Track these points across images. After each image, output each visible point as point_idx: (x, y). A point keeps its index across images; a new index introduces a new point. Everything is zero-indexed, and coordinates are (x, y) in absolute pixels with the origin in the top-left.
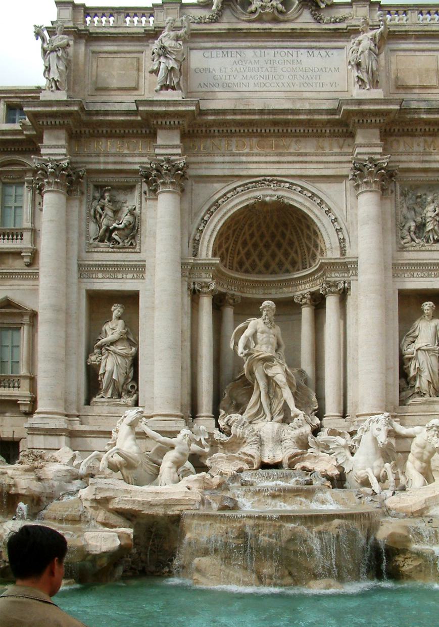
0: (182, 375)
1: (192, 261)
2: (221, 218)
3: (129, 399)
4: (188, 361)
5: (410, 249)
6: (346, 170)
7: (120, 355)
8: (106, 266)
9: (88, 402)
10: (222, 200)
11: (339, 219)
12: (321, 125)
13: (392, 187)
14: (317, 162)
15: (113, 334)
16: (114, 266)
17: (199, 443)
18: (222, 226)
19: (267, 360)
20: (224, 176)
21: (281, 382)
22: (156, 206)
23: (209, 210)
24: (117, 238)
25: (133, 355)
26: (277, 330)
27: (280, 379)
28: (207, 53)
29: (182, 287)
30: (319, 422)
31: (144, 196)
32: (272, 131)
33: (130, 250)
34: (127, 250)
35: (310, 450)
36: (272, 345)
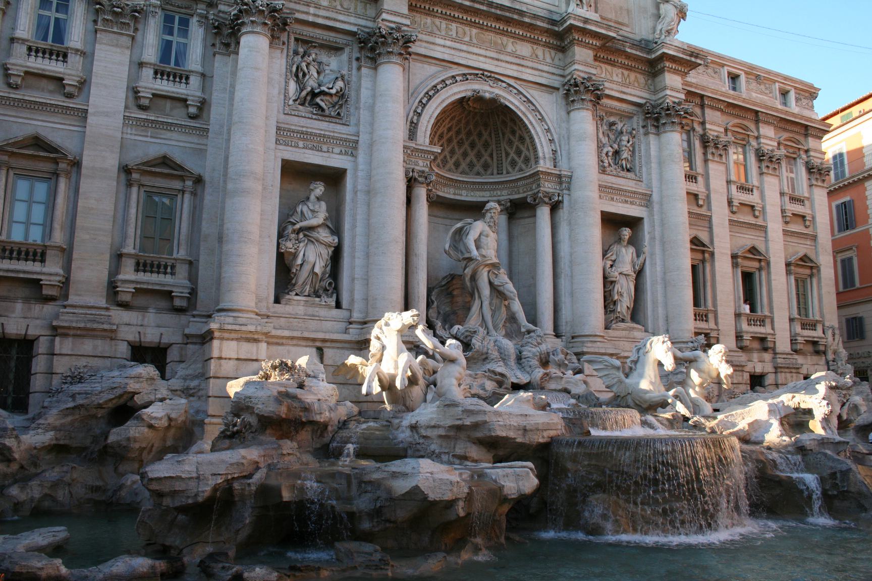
3: (330, 299)
6: (556, 82)
9: (277, 301)
10: (441, 86)
14: (533, 68)
16: (320, 135)
23: (427, 93)
24: (322, 104)
34: (334, 120)
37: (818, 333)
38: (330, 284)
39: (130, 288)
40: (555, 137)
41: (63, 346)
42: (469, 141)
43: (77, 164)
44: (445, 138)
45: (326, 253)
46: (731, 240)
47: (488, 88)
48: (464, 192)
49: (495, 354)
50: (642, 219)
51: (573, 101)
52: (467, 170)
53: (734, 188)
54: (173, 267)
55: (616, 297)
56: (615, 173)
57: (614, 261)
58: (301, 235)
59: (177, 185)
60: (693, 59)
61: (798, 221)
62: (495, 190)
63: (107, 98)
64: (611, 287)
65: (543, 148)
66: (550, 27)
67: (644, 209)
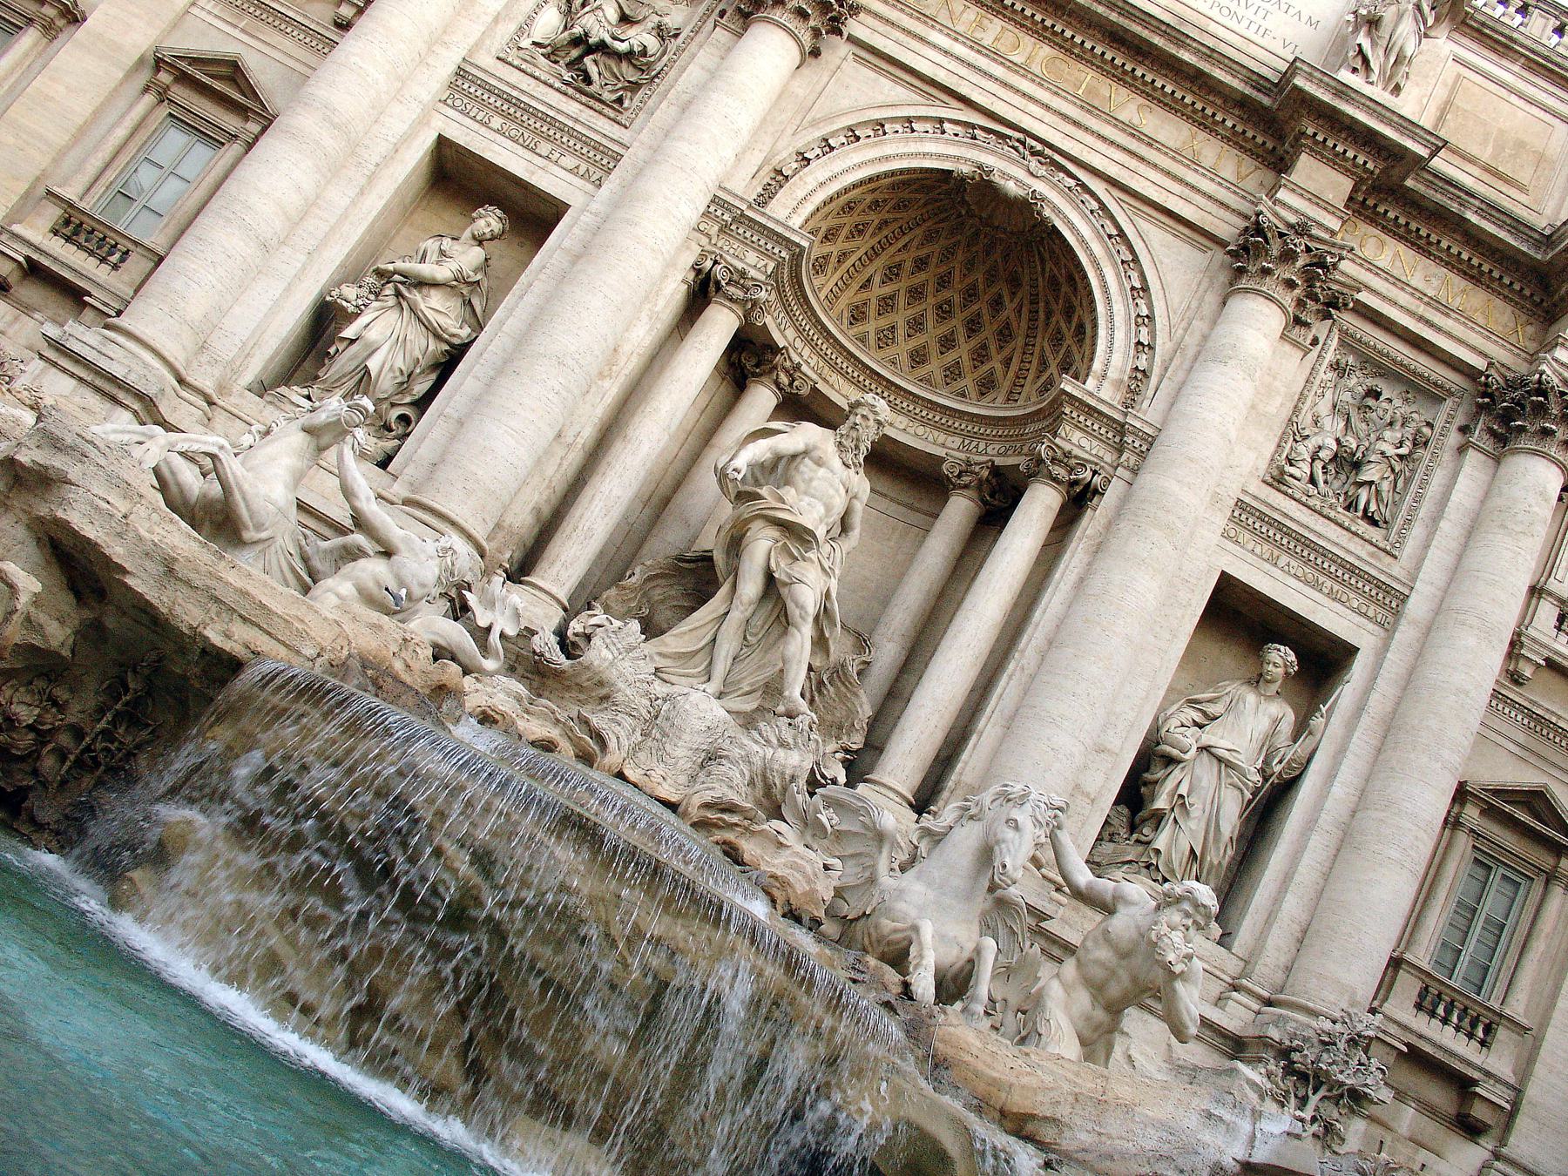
0: (548, 452)
1: (744, 207)
2: (872, 161)
4: (586, 432)
5: (1297, 496)
6: (1227, 227)
8: (527, 109)
9: (262, 389)
10: (898, 127)
11: (1158, 326)
12: (1219, 102)
13: (1320, 329)
14: (1168, 174)
15: (437, 263)
16: (544, 118)
17: (481, 635)
18: (861, 183)
19: (796, 534)
20: (933, 83)
21: (802, 608)
22: (729, 50)
24: (593, 70)
25: (456, 341)
26: (861, 483)
27: (802, 599)
29: (679, 250)
30: (842, 779)
31: (715, 16)
32: (1098, 51)
33: (607, 110)
34: (597, 106)
35: (776, 824)
36: (828, 508)
38: (404, 419)
39: (19, 253)
40: (1163, 345)
42: (966, 313)
44: (902, 285)
45: (423, 347)
47: (1020, 173)
50: (1351, 651)
51: (1241, 271)
52: (938, 376)
54: (122, 260)
55: (1161, 803)
58: (389, 290)
59: (230, 122)
62: (973, 436)
64: (1160, 774)
66: (1248, 91)
67: (1371, 626)
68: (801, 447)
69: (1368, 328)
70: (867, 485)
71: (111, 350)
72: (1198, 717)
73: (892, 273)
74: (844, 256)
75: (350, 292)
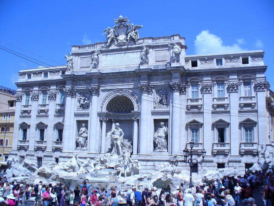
2: (108, 100)
7: (83, 137)
9: (76, 149)
17: (97, 161)
18: (109, 102)
19: (116, 139)
28: (107, 56)
37: (255, 147)
41: (45, 158)
43: (47, 126)
44: (120, 105)
46: (212, 118)
48: (127, 117)
49: (108, 160)
50: (168, 119)
52: (128, 111)
53: (215, 100)
55: (157, 143)
56: (159, 107)
57: (159, 132)
60: (178, 68)
61: (247, 107)
63: (52, 113)
65: (135, 105)
68: (113, 131)
69: (157, 86)
70: (121, 130)
71: (63, 154)
72: (157, 133)
73: (119, 105)
74: (113, 107)
75: (77, 137)
